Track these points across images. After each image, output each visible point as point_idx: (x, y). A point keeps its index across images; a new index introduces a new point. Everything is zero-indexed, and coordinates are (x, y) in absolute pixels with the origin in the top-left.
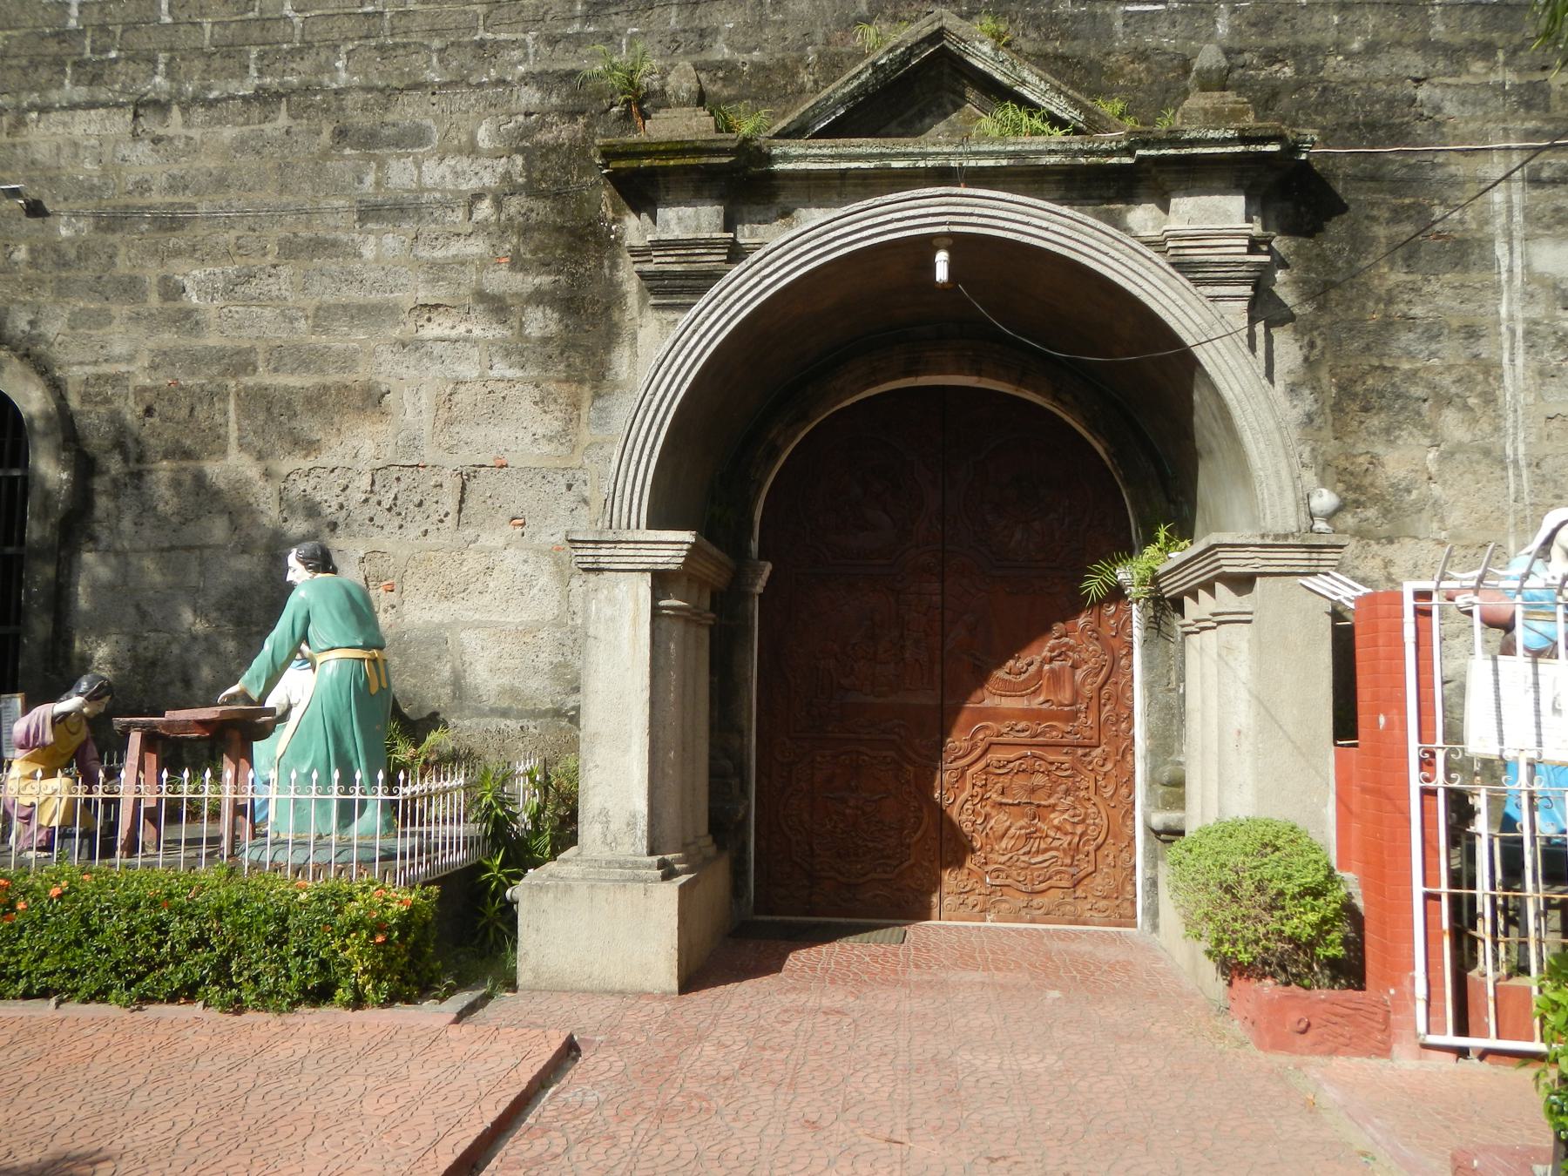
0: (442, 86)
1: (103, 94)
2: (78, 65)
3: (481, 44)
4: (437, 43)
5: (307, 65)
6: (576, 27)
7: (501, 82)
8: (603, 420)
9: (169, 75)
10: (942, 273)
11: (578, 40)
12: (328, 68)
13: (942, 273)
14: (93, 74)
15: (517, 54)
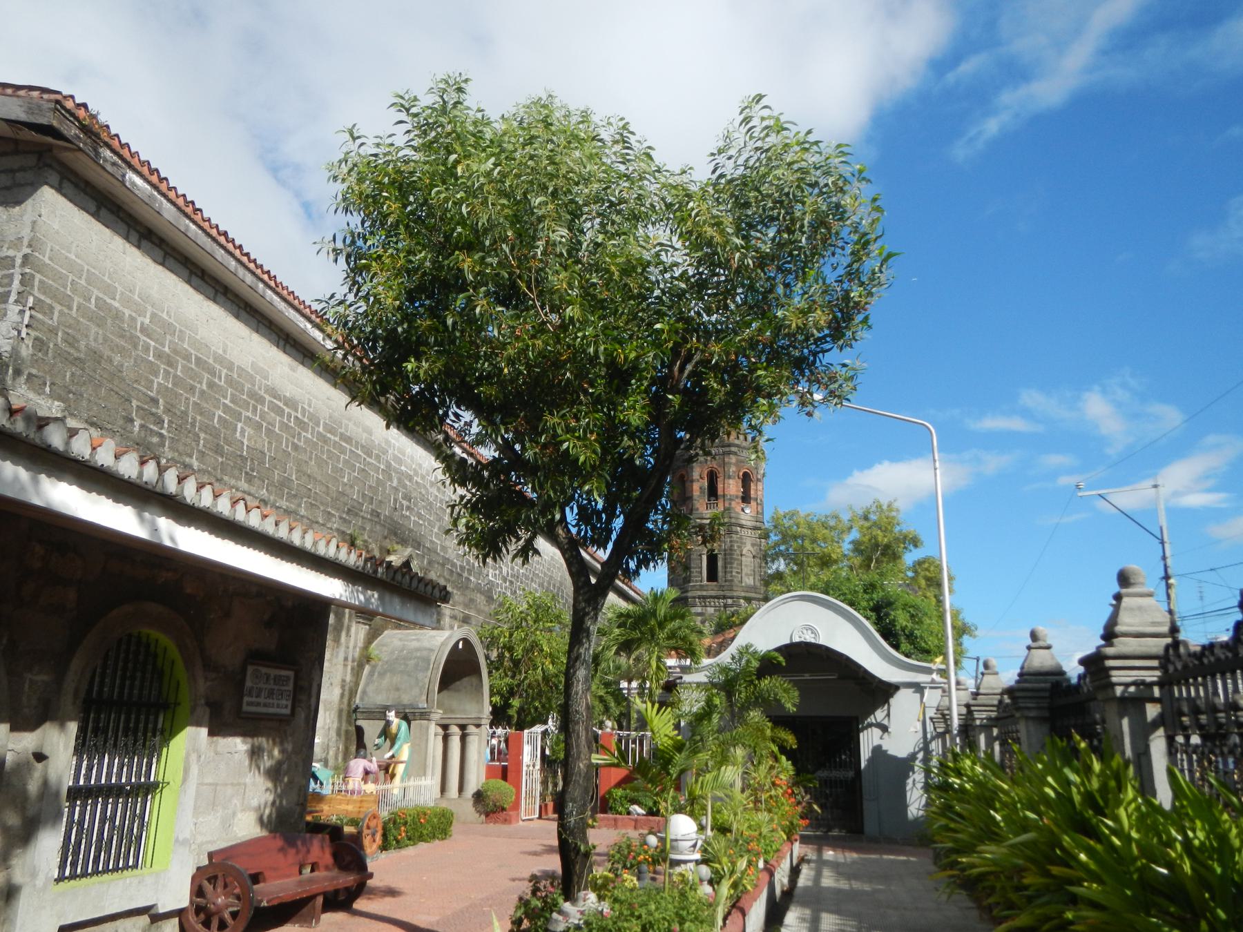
0: (323, 525)
1: (253, 490)
2: (247, 473)
3: (329, 513)
4: (322, 508)
5: (296, 501)
6: (344, 516)
7: (331, 529)
8: (337, 656)
9: (267, 490)
10: (460, 646)
11: (344, 519)
12: (299, 505)
13: (460, 646)
14: (250, 479)
15: (334, 519)
